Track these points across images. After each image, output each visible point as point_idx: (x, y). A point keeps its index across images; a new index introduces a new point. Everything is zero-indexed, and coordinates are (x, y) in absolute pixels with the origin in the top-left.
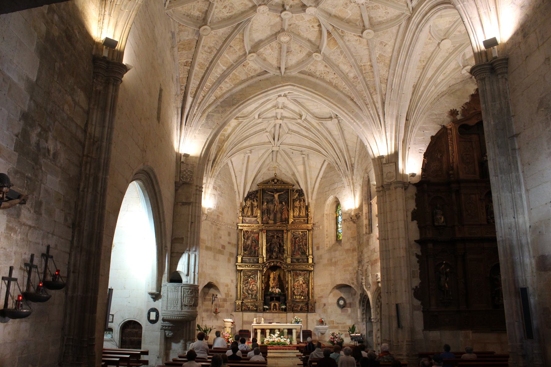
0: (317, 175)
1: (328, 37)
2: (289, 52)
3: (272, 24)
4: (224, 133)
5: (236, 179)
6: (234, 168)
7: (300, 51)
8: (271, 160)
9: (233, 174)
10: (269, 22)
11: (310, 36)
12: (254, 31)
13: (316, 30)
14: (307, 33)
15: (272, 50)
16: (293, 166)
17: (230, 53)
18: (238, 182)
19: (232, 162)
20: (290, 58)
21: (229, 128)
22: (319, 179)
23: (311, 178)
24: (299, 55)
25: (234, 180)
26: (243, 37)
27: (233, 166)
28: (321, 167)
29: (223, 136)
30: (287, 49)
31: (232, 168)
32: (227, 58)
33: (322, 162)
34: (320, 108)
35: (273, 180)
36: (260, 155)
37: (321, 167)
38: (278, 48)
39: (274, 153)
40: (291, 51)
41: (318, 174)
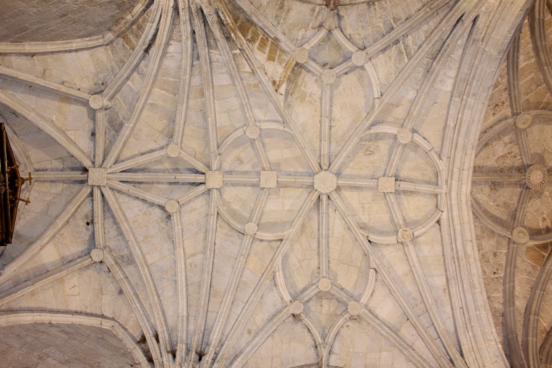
0: (49, 307)
1: (538, 246)
2: (494, 186)
3: (546, 156)
4: (258, 43)
5: (26, 54)
6: (61, 55)
7: (498, 205)
8: (36, 166)
9: (50, 47)
10: (550, 150)
11: (530, 218)
12: (542, 127)
13: (541, 224)
14: (533, 211)
15: (502, 157)
16: (55, 230)
17: (530, 84)
18: (13, 58)
19: (76, 51)
20: (483, 188)
21: (266, 56)
22: (46, 318)
23: (33, 294)
24: (492, 204)
25: (28, 47)
26: (541, 109)
27: (70, 51)
28: (76, 313)
29: (252, 37)
30: (499, 183)
31: (67, 47)
32: (527, 77)
33: (88, 311)
34: (301, 266)
35: (14, 174)
36: (69, 133)
37: (76, 313)
38: (502, 166)
39: (78, 175)
40: (496, 190)
41: (58, 312)
